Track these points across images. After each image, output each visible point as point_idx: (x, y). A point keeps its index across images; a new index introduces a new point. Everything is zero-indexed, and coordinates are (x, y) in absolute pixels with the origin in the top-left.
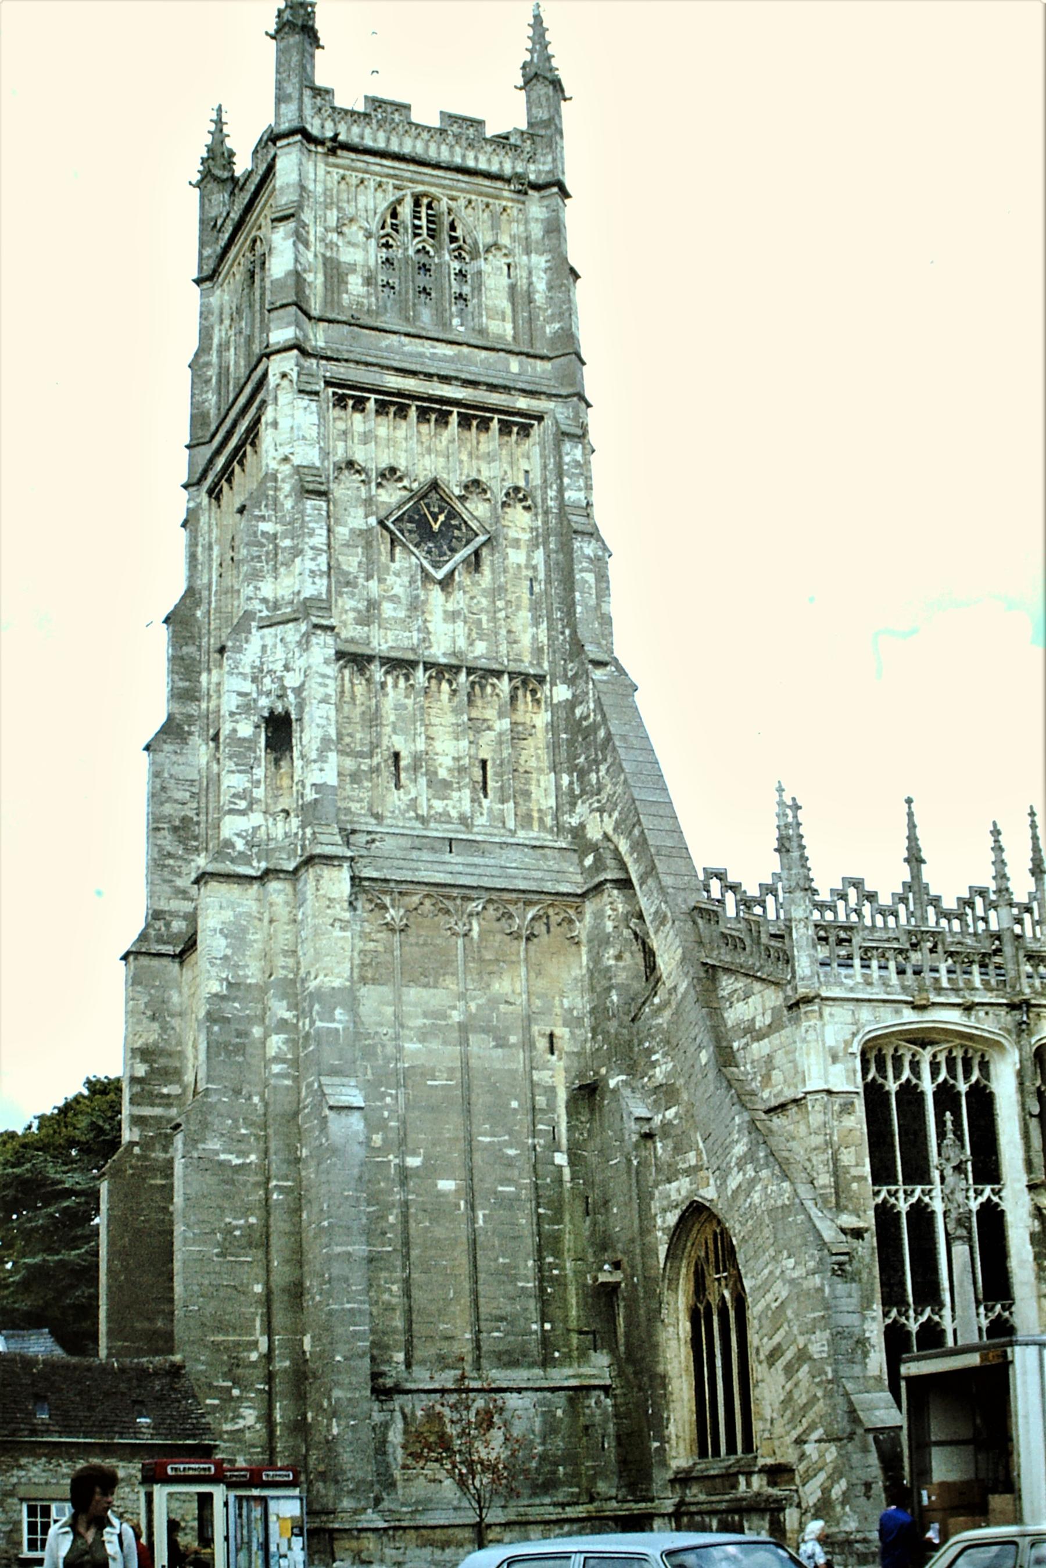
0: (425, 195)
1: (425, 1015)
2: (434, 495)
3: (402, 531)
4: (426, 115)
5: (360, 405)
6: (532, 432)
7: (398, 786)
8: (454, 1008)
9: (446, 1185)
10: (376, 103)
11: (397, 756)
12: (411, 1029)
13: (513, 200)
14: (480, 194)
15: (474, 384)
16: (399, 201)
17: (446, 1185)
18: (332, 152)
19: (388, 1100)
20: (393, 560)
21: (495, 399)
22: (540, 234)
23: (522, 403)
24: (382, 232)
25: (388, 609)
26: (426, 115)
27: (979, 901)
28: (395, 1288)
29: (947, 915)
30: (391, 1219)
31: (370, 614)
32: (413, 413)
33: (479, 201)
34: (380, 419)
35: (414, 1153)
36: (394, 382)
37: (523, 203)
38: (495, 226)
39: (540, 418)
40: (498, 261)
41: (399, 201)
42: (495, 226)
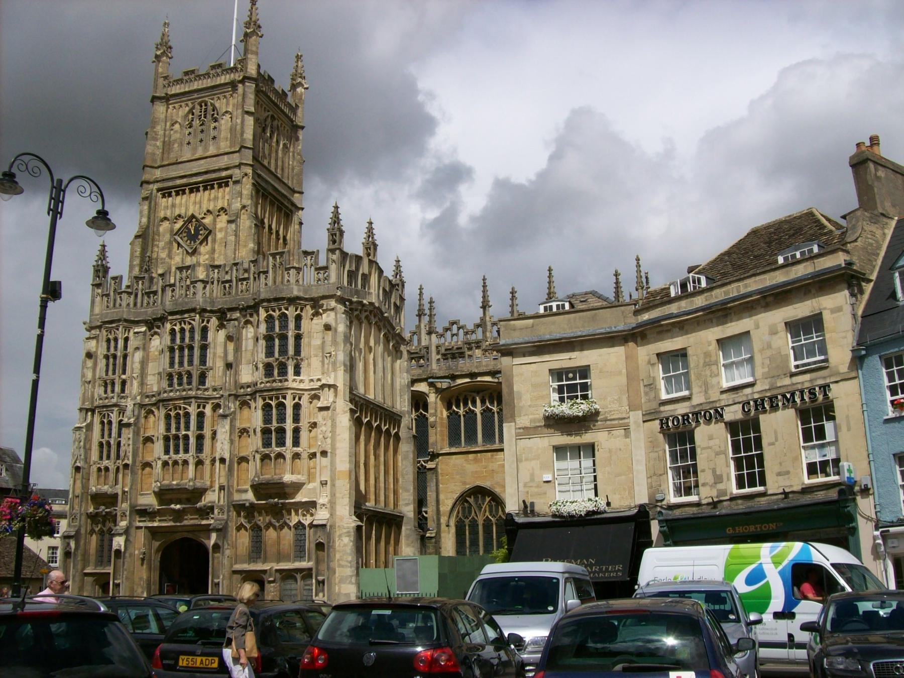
0: (202, 102)
2: (194, 220)
3: (181, 238)
5: (170, 195)
10: (186, 73)
15: (206, 173)
16: (193, 108)
21: (214, 176)
23: (224, 174)
33: (221, 96)
36: (179, 182)
38: (228, 104)
39: (231, 178)
40: (228, 116)
41: (193, 108)
42: (228, 104)
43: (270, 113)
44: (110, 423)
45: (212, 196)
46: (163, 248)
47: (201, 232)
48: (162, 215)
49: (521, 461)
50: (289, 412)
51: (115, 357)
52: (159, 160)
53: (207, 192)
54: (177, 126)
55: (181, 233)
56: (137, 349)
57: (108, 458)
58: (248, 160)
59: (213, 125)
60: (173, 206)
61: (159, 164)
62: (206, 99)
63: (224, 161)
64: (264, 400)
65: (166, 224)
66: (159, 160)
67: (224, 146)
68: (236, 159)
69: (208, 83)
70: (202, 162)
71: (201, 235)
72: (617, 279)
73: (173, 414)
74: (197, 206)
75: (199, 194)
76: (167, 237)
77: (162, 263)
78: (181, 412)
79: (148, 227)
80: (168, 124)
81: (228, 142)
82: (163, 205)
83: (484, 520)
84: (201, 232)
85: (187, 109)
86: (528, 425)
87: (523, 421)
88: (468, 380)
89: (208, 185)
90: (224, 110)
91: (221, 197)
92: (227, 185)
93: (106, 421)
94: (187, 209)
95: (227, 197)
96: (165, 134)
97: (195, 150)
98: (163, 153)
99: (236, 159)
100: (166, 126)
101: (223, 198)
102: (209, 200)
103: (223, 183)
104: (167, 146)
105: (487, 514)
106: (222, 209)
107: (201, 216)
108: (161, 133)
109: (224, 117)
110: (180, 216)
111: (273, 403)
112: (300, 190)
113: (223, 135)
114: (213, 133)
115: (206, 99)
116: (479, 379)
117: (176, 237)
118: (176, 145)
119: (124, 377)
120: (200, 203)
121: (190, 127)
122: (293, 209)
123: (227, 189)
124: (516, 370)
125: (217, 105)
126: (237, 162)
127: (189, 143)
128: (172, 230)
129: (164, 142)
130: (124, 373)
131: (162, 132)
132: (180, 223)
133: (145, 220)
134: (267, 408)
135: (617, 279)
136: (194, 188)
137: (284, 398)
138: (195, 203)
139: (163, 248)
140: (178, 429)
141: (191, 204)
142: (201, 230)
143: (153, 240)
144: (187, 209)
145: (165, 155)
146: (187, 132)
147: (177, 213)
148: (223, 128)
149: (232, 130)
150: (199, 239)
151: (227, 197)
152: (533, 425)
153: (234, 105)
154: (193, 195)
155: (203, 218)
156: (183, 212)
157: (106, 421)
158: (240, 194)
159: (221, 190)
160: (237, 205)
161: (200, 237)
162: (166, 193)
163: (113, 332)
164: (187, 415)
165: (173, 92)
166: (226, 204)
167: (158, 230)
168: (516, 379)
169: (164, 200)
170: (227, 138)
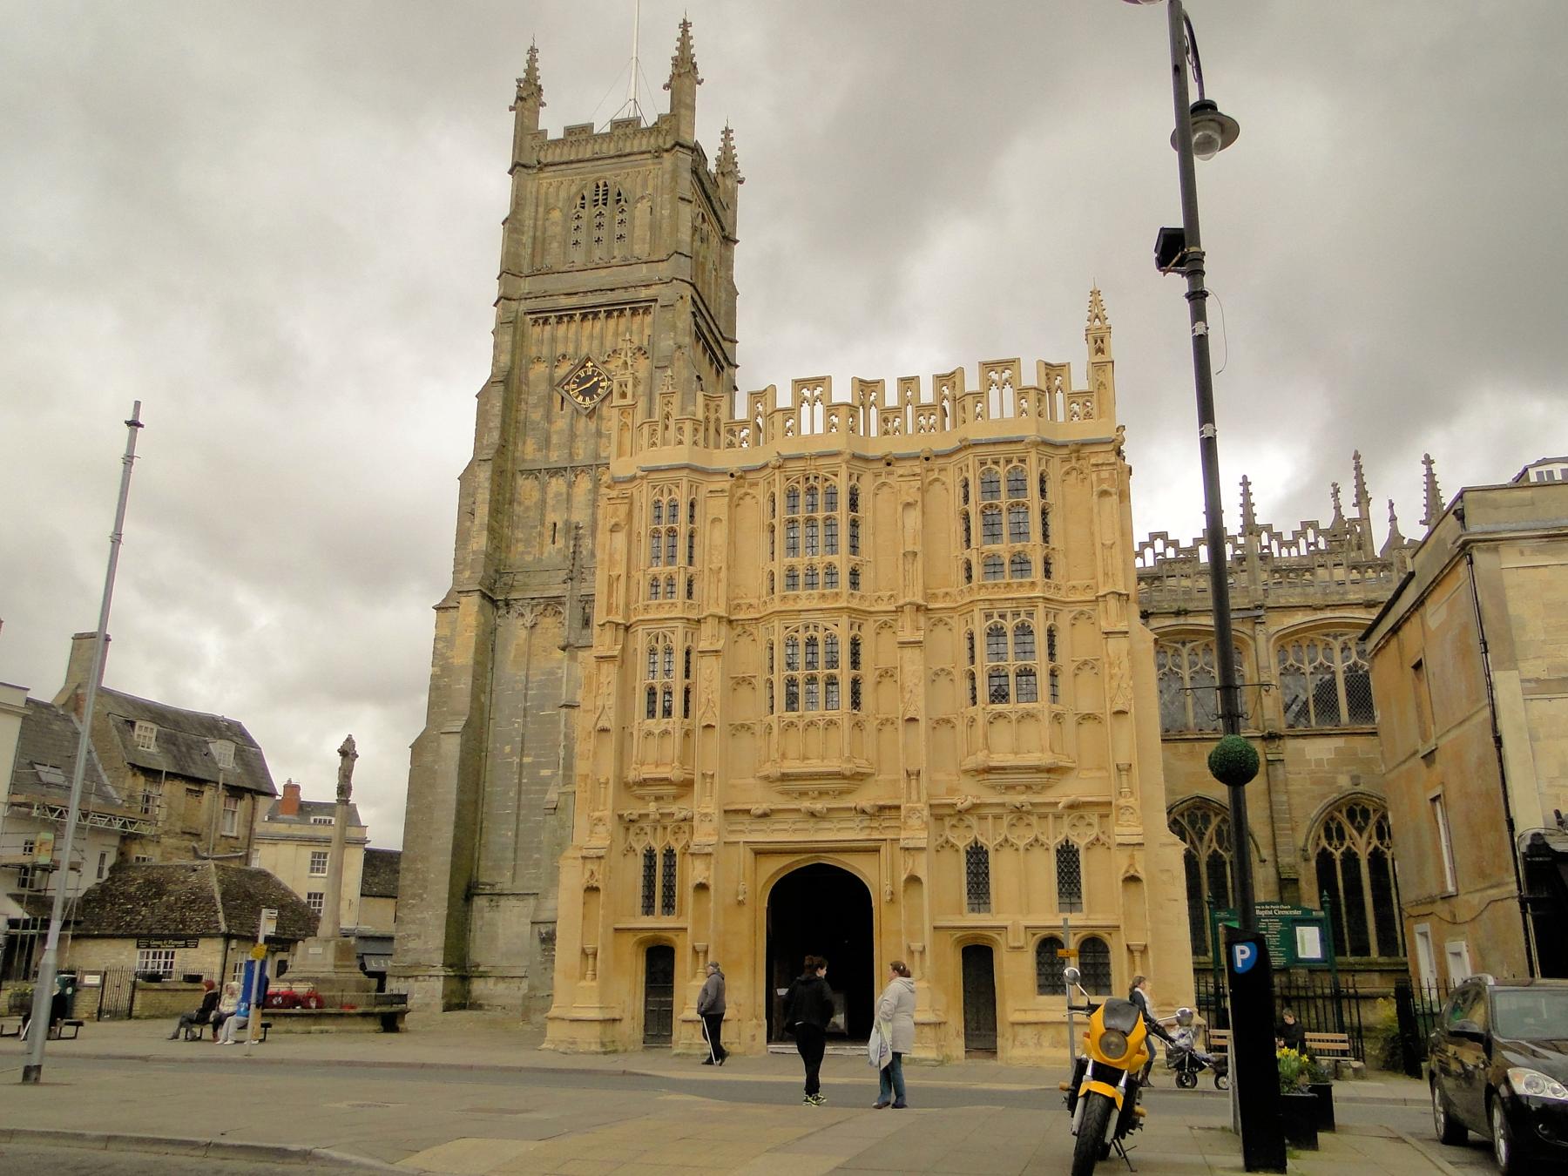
1: (543, 674)
2: (589, 364)
3: (568, 392)
4: (602, 126)
5: (546, 321)
6: (652, 310)
7: (554, 542)
8: (559, 668)
9: (545, 772)
11: (555, 524)
12: (533, 682)
13: (654, 164)
14: (632, 167)
16: (585, 187)
17: (545, 772)
18: (541, 169)
19: (516, 725)
20: (562, 409)
22: (669, 181)
23: (644, 293)
24: (574, 211)
25: (555, 439)
26: (602, 126)
27: (1310, 532)
28: (510, 834)
29: (1289, 545)
30: (512, 794)
31: (546, 443)
32: (553, 320)
34: (560, 326)
35: (528, 755)
37: (661, 163)
39: (656, 300)
40: (643, 206)
41: (585, 187)
43: (701, 210)
44: (669, 651)
45: (622, 328)
46: (535, 406)
47: (602, 384)
48: (534, 355)
49: (1538, 739)
50: (1041, 639)
51: (672, 533)
52: (525, 266)
53: (612, 322)
54: (556, 215)
55: (568, 384)
56: (716, 520)
57: (668, 712)
58: (684, 275)
59: (619, 217)
60: (553, 339)
61: (526, 271)
62: (608, 174)
63: (643, 271)
64: (988, 616)
65: (540, 370)
66: (525, 266)
67: (641, 249)
68: (664, 270)
69: (610, 148)
70: (603, 272)
71: (603, 388)
72: (1430, 469)
73: (802, 638)
74: (596, 343)
75: (598, 324)
76: (543, 388)
77: (533, 429)
78: (820, 636)
79: (512, 368)
80: (541, 210)
81: (647, 246)
82: (535, 336)
83: (1210, 856)
84: (602, 384)
85: (574, 189)
86: (1544, 676)
87: (1534, 668)
88: (1172, 621)
89: (613, 310)
90: (639, 195)
91: (638, 329)
92: (647, 310)
93: (660, 647)
94: (577, 348)
95: (647, 332)
96: (535, 224)
97: (589, 252)
98: (533, 255)
99: (664, 270)
100: (537, 211)
101: (642, 332)
102: (616, 334)
103: (639, 308)
104: (540, 244)
105: (1215, 845)
106: (640, 349)
107: (601, 359)
108: (529, 223)
109: (639, 205)
110: (564, 356)
111: (1009, 625)
112: (731, 337)
113: (637, 232)
114: (618, 231)
115: (608, 174)
116: (1191, 620)
117: (560, 389)
118: (555, 245)
119: (691, 569)
120: (602, 338)
121: (578, 218)
122: (725, 364)
123: (648, 319)
124: (1510, 579)
125: (628, 184)
126: (666, 275)
127: (576, 243)
128: (551, 379)
129: (534, 238)
130: (691, 562)
131: (531, 222)
132: (562, 371)
133: (505, 359)
134: (996, 633)
135: (1430, 469)
136: (589, 313)
137: (1030, 614)
138: (591, 336)
139: (535, 406)
140: (811, 664)
141: (584, 339)
142: (603, 380)
143: (520, 392)
144: (577, 348)
145: (538, 259)
146: (574, 225)
147: (560, 350)
148: (637, 222)
149: (654, 227)
150: (598, 395)
151: (647, 332)
152: (1554, 676)
153: (656, 188)
154: (588, 324)
155: (604, 363)
156: (571, 350)
157: (660, 647)
158: (674, 327)
159: (638, 319)
160: (666, 343)
161: (600, 390)
162: (541, 317)
163: (665, 490)
164: (832, 641)
165: (549, 159)
166: (645, 343)
167: (527, 377)
168: (1510, 593)
169: (537, 329)
170: (644, 239)
